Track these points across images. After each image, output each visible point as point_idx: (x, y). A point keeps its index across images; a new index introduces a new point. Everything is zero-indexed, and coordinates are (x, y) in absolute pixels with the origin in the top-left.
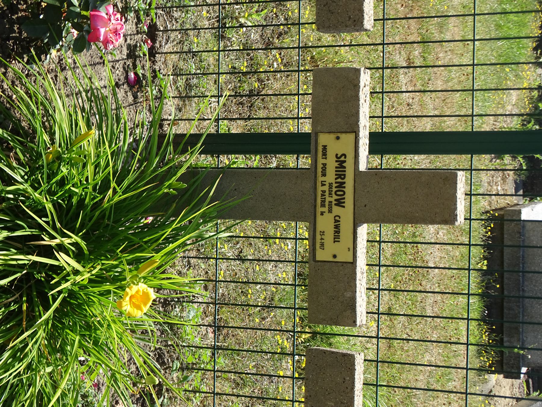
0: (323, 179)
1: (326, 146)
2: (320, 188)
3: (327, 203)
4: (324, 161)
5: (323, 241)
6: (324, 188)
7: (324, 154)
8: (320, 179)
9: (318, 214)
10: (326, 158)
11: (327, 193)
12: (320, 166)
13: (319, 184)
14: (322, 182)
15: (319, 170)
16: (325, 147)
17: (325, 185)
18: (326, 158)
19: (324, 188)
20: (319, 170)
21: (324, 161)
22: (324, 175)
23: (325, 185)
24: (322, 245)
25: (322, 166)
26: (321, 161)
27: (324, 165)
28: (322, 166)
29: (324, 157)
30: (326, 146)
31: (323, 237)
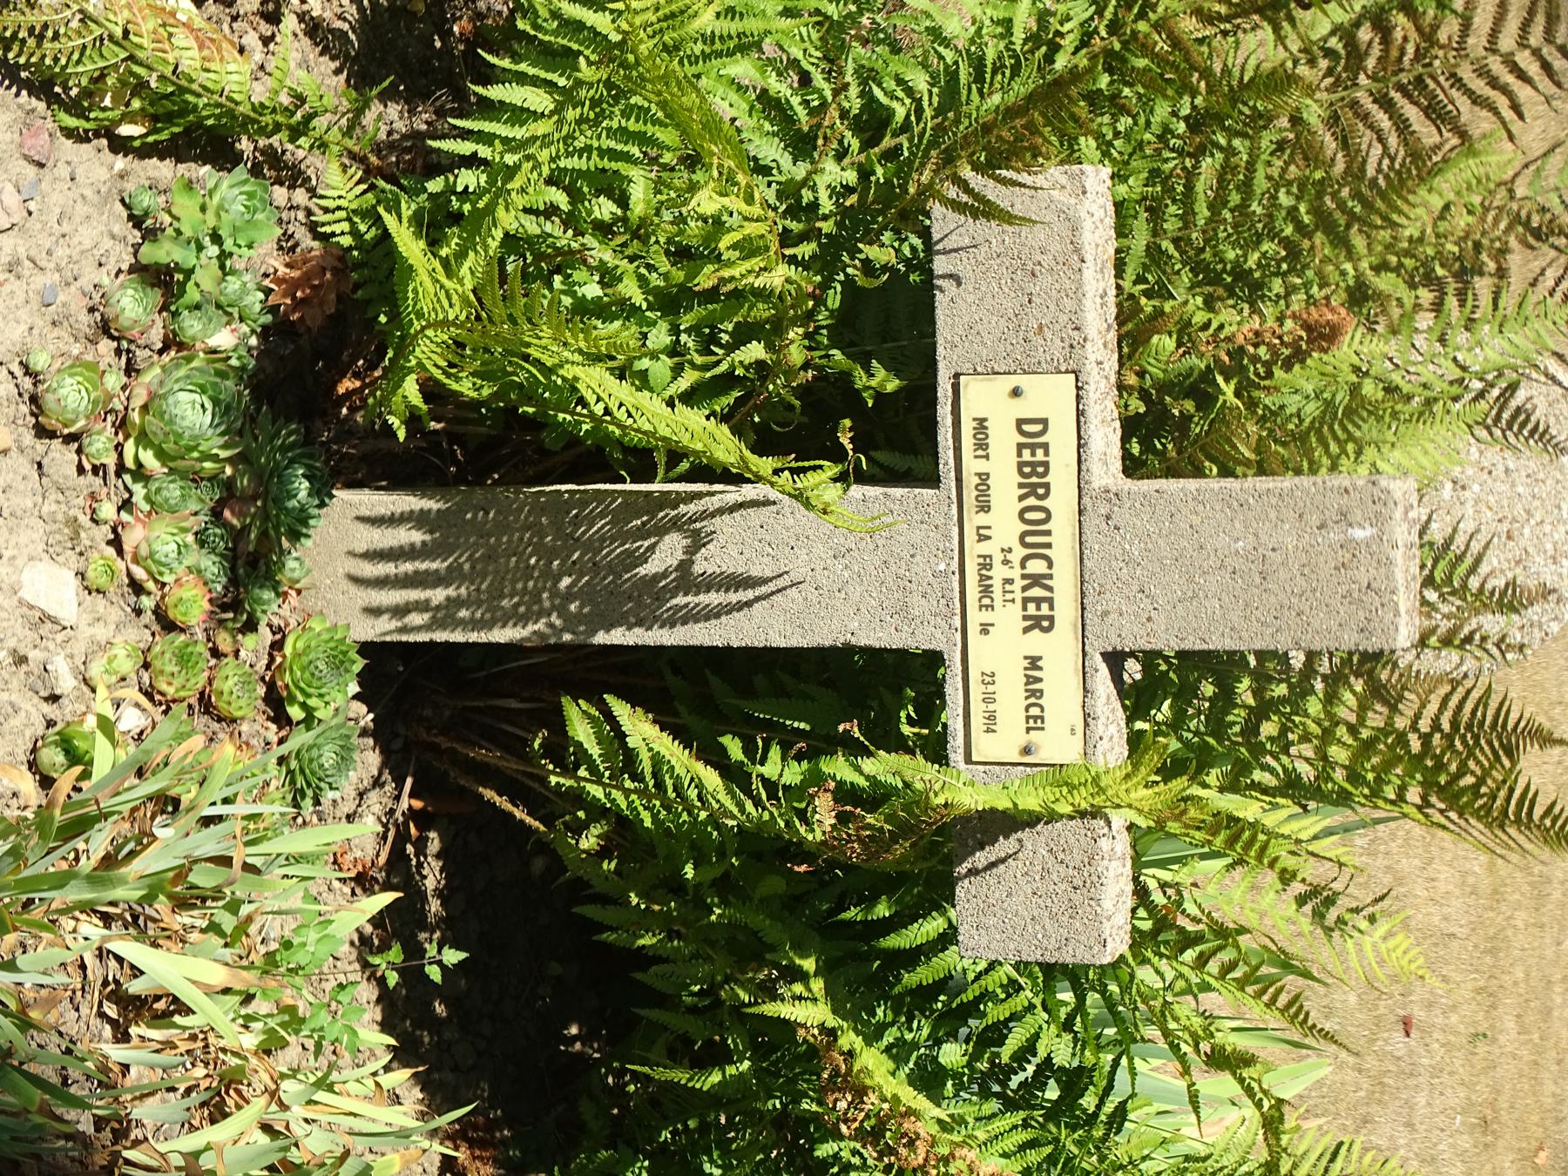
0: (982, 519)
1: (985, 420)
2: (973, 549)
4: (982, 466)
5: (991, 707)
6: (984, 548)
7: (982, 445)
8: (973, 520)
10: (987, 457)
12: (970, 481)
14: (979, 528)
16: (981, 424)
17: (989, 538)
18: (987, 457)
19: (984, 548)
20: (970, 495)
21: (982, 466)
22: (985, 508)
23: (989, 538)
24: (991, 717)
25: (977, 480)
26: (971, 465)
27: (984, 477)
28: (977, 480)
29: (980, 452)
30: (985, 420)
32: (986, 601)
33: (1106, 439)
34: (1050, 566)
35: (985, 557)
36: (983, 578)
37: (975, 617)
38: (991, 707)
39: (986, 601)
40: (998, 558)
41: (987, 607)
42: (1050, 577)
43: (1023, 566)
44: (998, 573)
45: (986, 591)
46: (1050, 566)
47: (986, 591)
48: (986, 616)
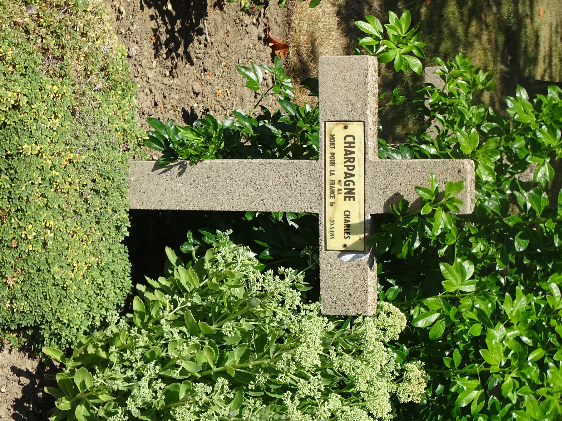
0: (332, 168)
1: (334, 135)
2: (328, 177)
3: (336, 193)
4: (333, 151)
5: (333, 230)
6: (333, 177)
7: (332, 144)
8: (329, 168)
9: (328, 204)
10: (334, 147)
11: (336, 182)
12: (328, 155)
13: (328, 174)
14: (330, 171)
15: (328, 160)
16: (332, 137)
18: (334, 147)
19: (333, 177)
20: (328, 160)
22: (333, 164)
24: (333, 234)
27: (333, 154)
28: (330, 155)
29: (332, 146)
30: (334, 135)
31: (333, 226)
32: (332, 195)
33: (373, 141)
34: (354, 139)
35: (332, 180)
36: (331, 187)
37: (329, 200)
38: (333, 230)
39: (332, 195)
40: (336, 182)
41: (332, 197)
42: (354, 143)
43: (345, 139)
44: (337, 186)
45: (332, 192)
46: (354, 139)
47: (332, 192)
48: (332, 200)
